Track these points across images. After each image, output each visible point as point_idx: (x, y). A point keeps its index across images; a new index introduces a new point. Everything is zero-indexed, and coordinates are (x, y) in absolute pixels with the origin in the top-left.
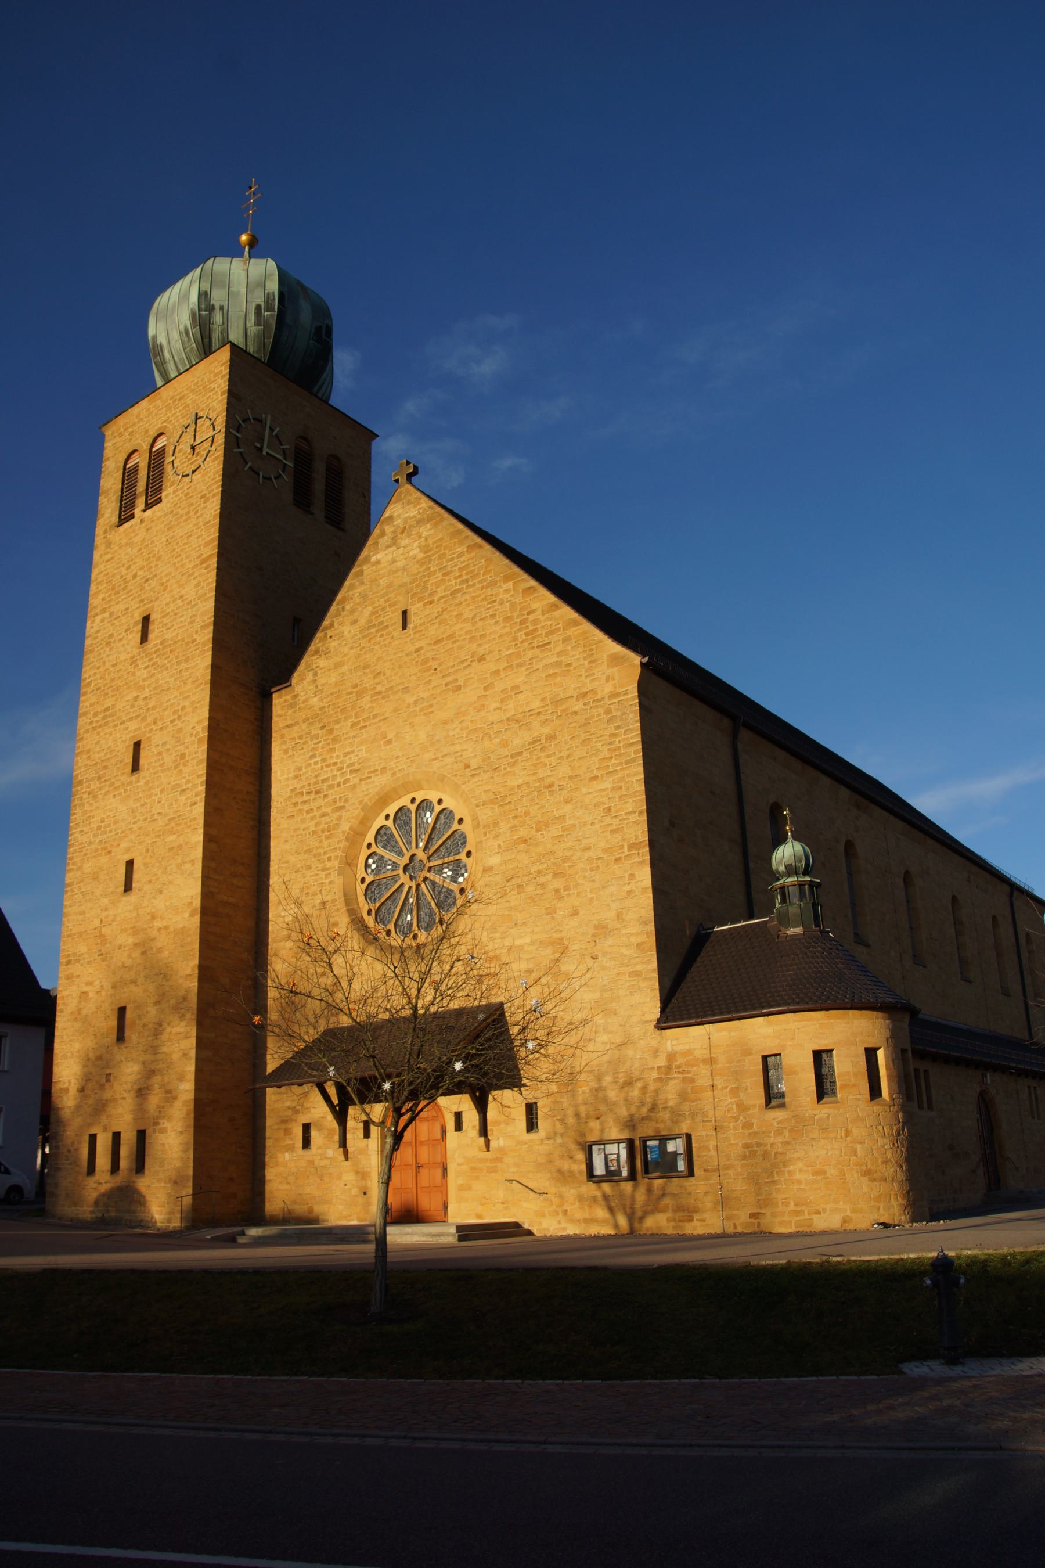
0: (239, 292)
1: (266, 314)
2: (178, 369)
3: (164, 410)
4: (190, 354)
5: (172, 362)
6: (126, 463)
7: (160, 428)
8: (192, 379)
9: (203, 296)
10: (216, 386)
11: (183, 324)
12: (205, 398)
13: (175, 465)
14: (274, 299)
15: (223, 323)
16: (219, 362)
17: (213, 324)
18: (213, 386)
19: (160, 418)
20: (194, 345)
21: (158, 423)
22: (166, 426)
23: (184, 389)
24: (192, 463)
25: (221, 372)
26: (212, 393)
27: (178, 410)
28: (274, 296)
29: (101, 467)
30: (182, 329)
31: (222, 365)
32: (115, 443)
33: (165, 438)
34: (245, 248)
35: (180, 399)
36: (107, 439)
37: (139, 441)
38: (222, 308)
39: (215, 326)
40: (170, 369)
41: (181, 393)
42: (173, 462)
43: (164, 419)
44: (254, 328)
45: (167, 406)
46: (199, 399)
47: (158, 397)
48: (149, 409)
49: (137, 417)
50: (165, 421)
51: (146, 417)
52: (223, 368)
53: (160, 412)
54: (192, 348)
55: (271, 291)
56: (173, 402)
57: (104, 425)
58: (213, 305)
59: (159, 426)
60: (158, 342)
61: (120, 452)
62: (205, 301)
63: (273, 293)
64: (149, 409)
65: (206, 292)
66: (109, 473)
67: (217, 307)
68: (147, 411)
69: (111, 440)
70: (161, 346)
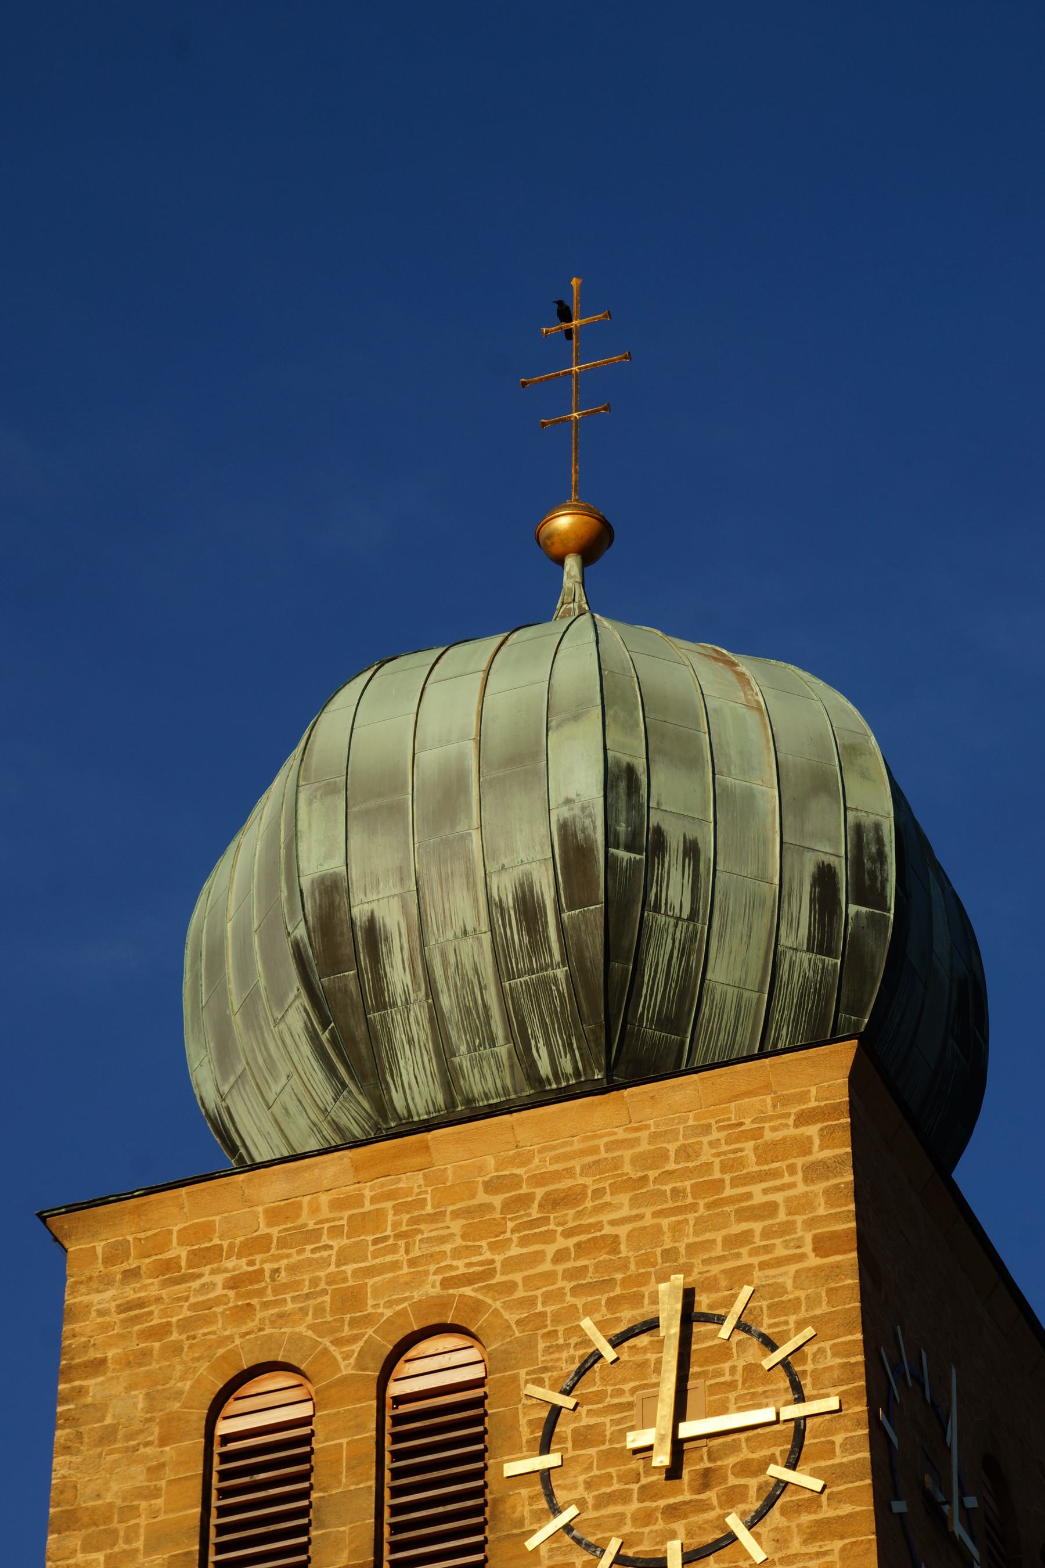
0: (750, 797)
1: (853, 909)
2: (443, 1052)
3: (456, 1226)
4: (525, 1002)
5: (419, 1012)
6: (215, 1411)
7: (443, 1304)
8: (621, 1134)
9: (623, 785)
10: (778, 1197)
11: (517, 873)
12: (718, 1236)
13: (560, 1496)
14: (881, 856)
15: (693, 916)
16: (786, 1101)
17: (657, 909)
18: (758, 1194)
19: (432, 1257)
20: (560, 973)
21: (416, 1280)
22: (478, 1307)
23: (577, 1164)
24: (673, 1512)
25: (804, 1146)
26: (757, 1226)
27: (551, 1250)
28: (880, 841)
29: (53, 1399)
30: (505, 888)
31: (803, 1119)
32: (141, 1304)
33: (474, 1354)
34: (560, 561)
35: (554, 1202)
36: (74, 1273)
37: (302, 1329)
38: (691, 850)
39: (661, 919)
40: (399, 1036)
41: (557, 1176)
42: (545, 1476)
43: (461, 1267)
44: (806, 956)
45: (468, 1212)
46: (677, 1229)
47: (417, 1160)
48: (357, 1200)
49: (274, 1215)
50: (468, 1280)
51: (336, 1231)
52: (813, 1130)
53: (428, 1230)
54: (545, 984)
55: (868, 821)
56: (507, 1207)
57: (72, 1208)
58: (659, 832)
59: (431, 1288)
60: (359, 912)
61: (176, 1349)
62: (630, 807)
63: (877, 827)
64: (357, 1200)
65: (630, 770)
66: (108, 1435)
67: (674, 842)
68: (338, 1204)
69: (107, 1281)
70: (373, 934)
